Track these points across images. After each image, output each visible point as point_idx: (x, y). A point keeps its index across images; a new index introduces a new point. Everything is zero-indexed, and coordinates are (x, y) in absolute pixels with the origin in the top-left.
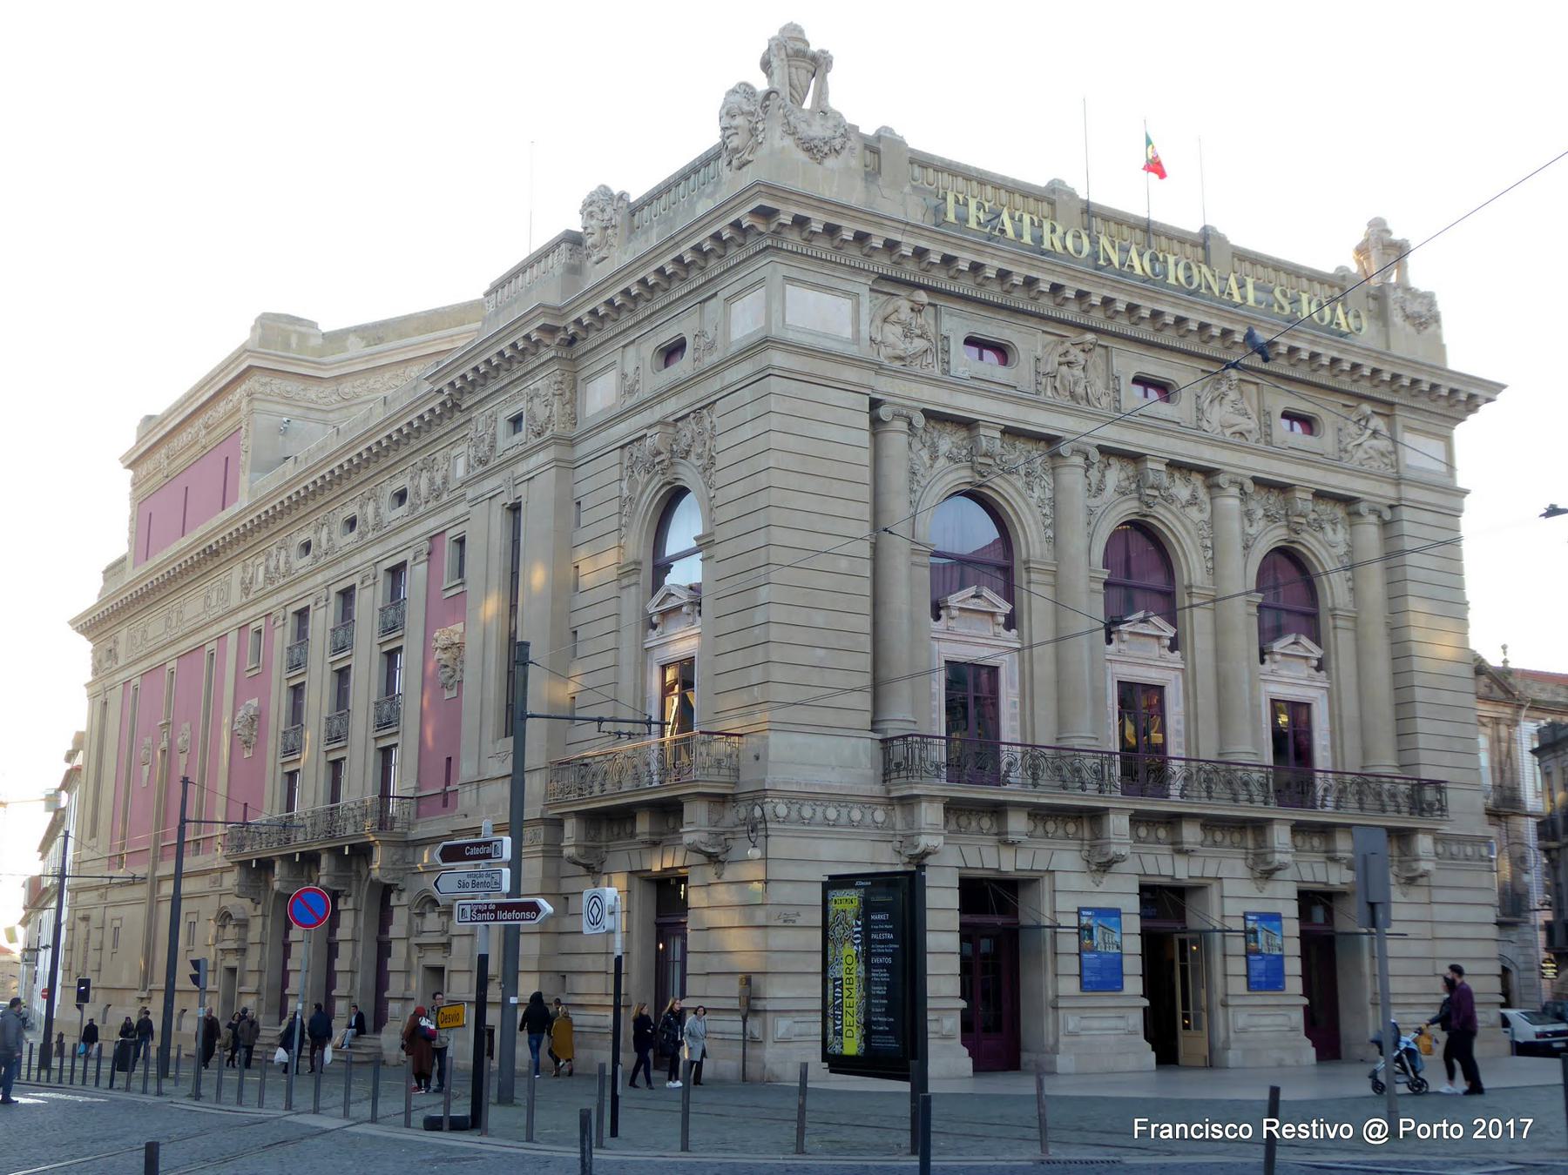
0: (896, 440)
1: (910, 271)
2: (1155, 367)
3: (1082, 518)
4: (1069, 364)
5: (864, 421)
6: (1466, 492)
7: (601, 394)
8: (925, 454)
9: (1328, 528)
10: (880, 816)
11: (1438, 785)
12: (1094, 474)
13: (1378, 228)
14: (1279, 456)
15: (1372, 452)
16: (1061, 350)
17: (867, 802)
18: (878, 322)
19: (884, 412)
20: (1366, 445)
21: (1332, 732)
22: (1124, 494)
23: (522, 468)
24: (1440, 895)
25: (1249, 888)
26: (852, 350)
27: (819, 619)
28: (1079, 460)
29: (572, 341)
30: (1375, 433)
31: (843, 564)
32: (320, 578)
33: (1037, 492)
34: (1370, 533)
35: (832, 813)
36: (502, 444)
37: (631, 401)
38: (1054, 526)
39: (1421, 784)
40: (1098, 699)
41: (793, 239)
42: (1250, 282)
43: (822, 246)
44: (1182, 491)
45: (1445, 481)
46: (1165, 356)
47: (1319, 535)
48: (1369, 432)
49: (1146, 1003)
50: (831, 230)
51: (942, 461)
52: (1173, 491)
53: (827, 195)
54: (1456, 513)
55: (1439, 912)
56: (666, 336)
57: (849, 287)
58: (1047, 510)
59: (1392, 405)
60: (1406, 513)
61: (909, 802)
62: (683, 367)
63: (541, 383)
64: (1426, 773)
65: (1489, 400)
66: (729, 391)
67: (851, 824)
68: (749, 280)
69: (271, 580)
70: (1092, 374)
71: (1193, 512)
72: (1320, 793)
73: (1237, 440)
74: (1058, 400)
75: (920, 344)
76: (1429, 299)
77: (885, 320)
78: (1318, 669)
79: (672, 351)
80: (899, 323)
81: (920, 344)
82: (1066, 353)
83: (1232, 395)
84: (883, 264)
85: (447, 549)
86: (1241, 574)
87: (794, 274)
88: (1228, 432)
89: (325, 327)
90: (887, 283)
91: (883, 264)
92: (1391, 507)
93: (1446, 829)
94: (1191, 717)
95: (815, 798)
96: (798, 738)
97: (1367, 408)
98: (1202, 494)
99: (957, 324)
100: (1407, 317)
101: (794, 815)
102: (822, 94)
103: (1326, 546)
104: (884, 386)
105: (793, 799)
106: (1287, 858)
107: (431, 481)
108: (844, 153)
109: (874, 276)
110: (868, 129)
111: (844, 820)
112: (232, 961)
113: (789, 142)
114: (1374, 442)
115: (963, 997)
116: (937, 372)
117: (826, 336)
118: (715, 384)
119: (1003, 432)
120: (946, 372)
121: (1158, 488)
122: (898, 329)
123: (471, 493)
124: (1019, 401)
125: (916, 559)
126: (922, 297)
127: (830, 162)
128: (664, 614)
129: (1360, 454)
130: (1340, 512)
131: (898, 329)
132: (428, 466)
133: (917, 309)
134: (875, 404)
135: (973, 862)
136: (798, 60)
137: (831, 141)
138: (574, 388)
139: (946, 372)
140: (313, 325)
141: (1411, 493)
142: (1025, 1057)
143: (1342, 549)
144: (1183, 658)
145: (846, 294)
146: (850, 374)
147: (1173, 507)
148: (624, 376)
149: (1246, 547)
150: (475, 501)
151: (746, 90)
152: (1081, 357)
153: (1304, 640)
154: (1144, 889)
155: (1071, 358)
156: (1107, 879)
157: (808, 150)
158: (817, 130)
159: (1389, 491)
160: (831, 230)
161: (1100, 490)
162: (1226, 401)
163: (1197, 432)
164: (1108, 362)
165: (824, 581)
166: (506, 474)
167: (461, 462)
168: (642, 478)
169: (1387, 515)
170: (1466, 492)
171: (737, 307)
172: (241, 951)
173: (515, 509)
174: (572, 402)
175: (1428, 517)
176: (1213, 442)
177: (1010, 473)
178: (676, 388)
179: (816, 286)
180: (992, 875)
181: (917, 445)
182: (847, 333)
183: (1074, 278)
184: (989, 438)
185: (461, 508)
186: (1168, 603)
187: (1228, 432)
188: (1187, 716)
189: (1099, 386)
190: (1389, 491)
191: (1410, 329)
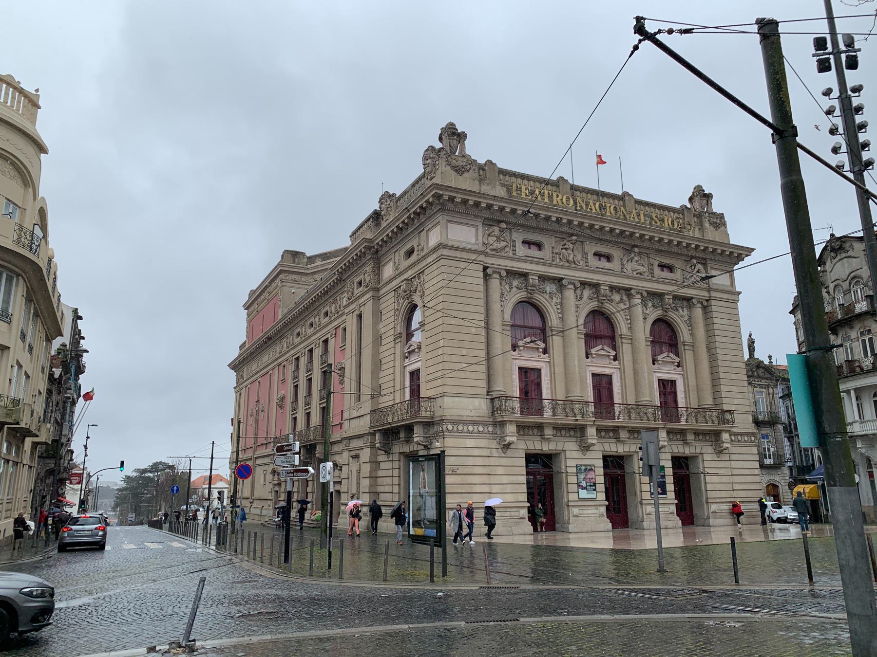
0: (495, 283)
1: (497, 216)
3: (573, 309)
4: (566, 249)
5: (481, 274)
6: (740, 293)
7: (388, 271)
8: (507, 287)
9: (680, 310)
10: (491, 429)
11: (730, 412)
12: (578, 291)
14: (657, 282)
16: (562, 243)
17: (485, 424)
18: (486, 236)
19: (489, 271)
21: (685, 391)
23: (362, 300)
24: (733, 457)
25: (575, 454)
26: (476, 247)
27: (464, 352)
28: (571, 286)
29: (377, 251)
30: (698, 272)
32: (302, 345)
33: (555, 300)
34: (698, 312)
35: (471, 428)
36: (356, 292)
37: (397, 272)
38: (562, 313)
39: (724, 412)
40: (583, 381)
41: (450, 206)
42: (642, 213)
43: (461, 208)
44: (616, 297)
45: (730, 289)
46: (606, 243)
48: (696, 269)
49: (528, 505)
50: (465, 202)
51: (514, 289)
52: (613, 297)
53: (464, 188)
54: (736, 302)
55: (734, 464)
56: (407, 247)
57: (473, 223)
58: (559, 306)
59: (705, 259)
60: (713, 302)
61: (502, 424)
62: (414, 257)
63: (368, 268)
64: (725, 408)
65: (747, 256)
66: (428, 266)
67: (479, 432)
68: (435, 223)
69: (288, 347)
70: (576, 252)
72: (617, 413)
73: (639, 275)
74: (562, 263)
75: (503, 244)
76: (721, 216)
77: (489, 235)
78: (678, 366)
79: (410, 253)
80: (494, 236)
81: (503, 244)
83: (636, 258)
84: (487, 214)
85: (340, 331)
86: (643, 331)
87: (451, 219)
89: (308, 255)
90: (490, 222)
91: (487, 214)
92: (707, 300)
93: (735, 430)
94: (624, 387)
95: (465, 423)
96: (457, 399)
97: (695, 261)
98: (625, 298)
99: (518, 236)
100: (711, 224)
101: (455, 429)
102: (463, 149)
103: (679, 318)
104: (489, 261)
105: (455, 422)
106: (666, 443)
107: (336, 307)
110: (482, 161)
111: (476, 430)
112: (277, 488)
113: (448, 168)
115: (528, 502)
116: (511, 254)
118: (424, 263)
119: (539, 277)
120: (514, 254)
121: (606, 296)
122: (495, 239)
123: (346, 311)
124: (545, 264)
125: (505, 328)
126: (504, 225)
127: (466, 175)
128: (409, 353)
130: (685, 303)
131: (495, 239)
132: (335, 302)
133: (502, 230)
134: (485, 268)
135: (531, 447)
137: (464, 166)
138: (379, 270)
139: (514, 254)
140: (303, 254)
141: (714, 294)
142: (557, 525)
143: (686, 318)
144: (549, 357)
145: (473, 226)
148: (395, 263)
149: (645, 318)
150: (348, 314)
151: (431, 148)
152: (571, 246)
153: (671, 355)
154: (604, 456)
156: (588, 453)
157: (456, 171)
158: (460, 163)
160: (465, 202)
161: (581, 298)
163: (622, 274)
164: (583, 248)
165: (466, 337)
166: (356, 303)
167: (345, 300)
168: (401, 301)
169: (705, 303)
170: (740, 293)
171: (431, 233)
172: (279, 485)
173: (360, 316)
174: (378, 274)
175: (723, 304)
176: (628, 277)
178: (411, 267)
179: (460, 223)
180: (540, 452)
181: (503, 283)
182: (473, 241)
183: (566, 215)
184: (533, 280)
185: (344, 317)
186: (543, 332)
188: (622, 386)
189: (579, 257)
190: (706, 294)
191: (712, 228)
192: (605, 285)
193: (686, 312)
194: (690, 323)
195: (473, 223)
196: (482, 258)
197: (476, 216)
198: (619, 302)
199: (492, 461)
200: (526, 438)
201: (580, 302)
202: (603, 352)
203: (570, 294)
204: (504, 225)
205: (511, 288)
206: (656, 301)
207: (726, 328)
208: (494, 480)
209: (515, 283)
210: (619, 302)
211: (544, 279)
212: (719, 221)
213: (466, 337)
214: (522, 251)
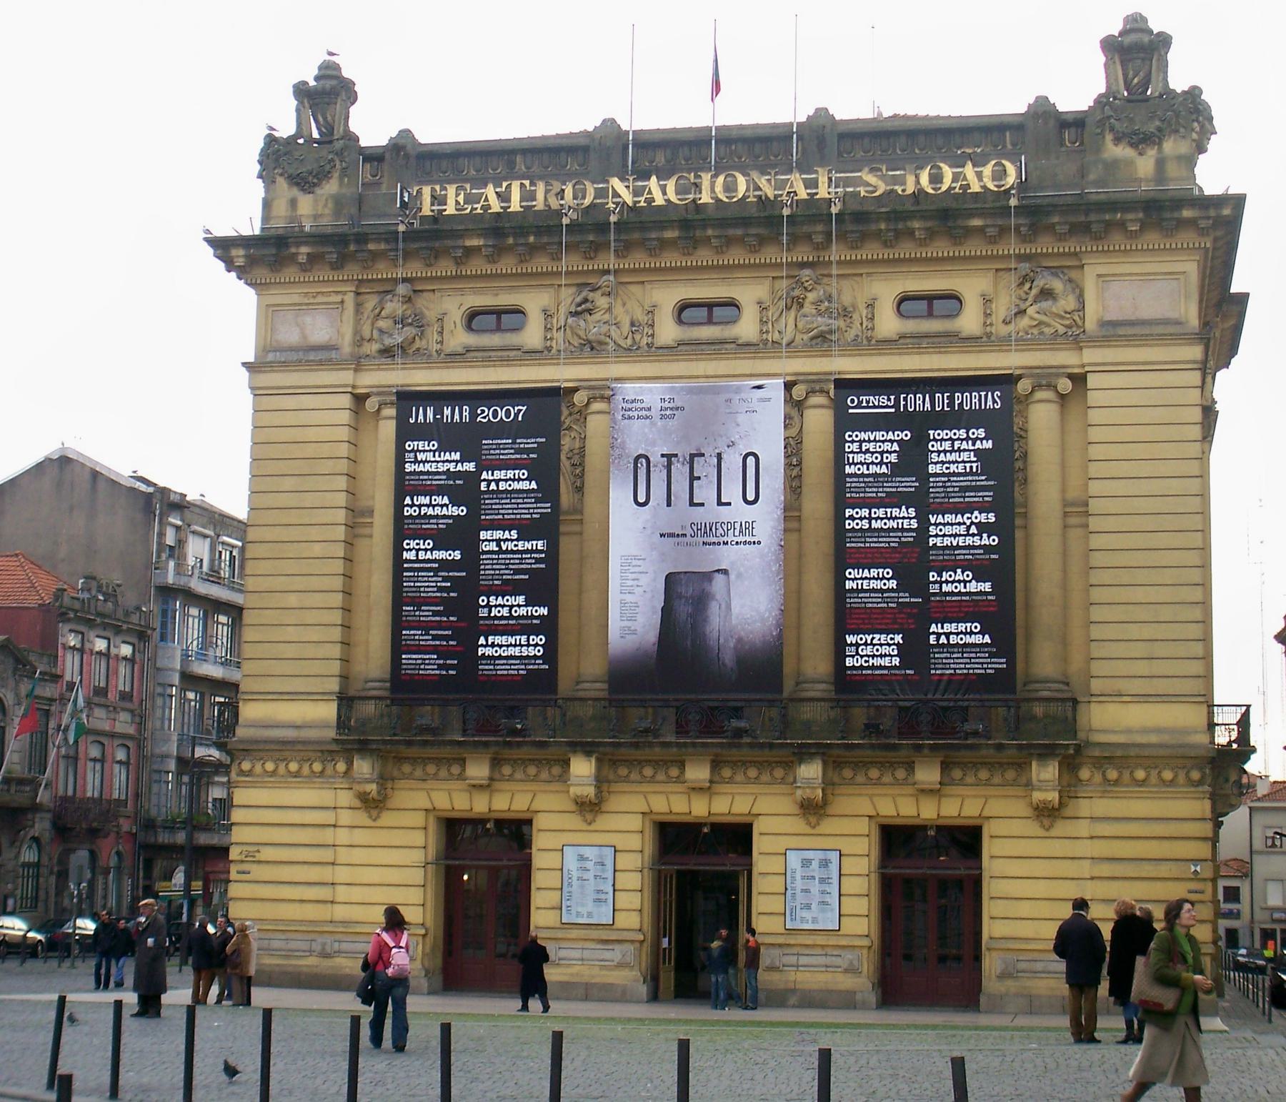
4: (590, 312)
5: (345, 417)
13: (1136, 24)
15: (1044, 318)
16: (578, 299)
19: (371, 404)
30: (1046, 294)
31: (317, 550)
48: (1034, 291)
59: (1075, 254)
82: (586, 300)
114: (1045, 305)
126: (402, 289)
129: (1024, 322)
136: (327, 94)
152: (602, 302)
155: (588, 305)
196: (346, 377)
199: (343, 836)
200: (430, 784)
204: (402, 289)
208: (342, 874)
212: (1190, 117)
214: (459, 338)
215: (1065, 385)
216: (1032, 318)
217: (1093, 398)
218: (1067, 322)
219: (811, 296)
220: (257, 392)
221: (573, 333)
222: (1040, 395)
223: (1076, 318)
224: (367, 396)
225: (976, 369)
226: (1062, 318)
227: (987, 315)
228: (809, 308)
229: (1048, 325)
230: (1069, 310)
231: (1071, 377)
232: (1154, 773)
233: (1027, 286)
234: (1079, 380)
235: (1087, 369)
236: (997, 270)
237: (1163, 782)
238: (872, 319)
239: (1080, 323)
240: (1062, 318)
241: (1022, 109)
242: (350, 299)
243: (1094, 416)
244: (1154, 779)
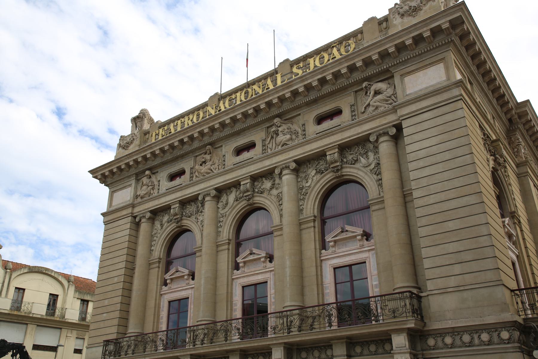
1: (141, 167)
2: (242, 141)
4: (205, 162)
20: (371, 104)
22: (237, 200)
27: (106, 302)
30: (377, 93)
31: (116, 280)
44: (267, 184)
47: (357, 165)
48: (372, 93)
51: (166, 224)
57: (129, 183)
59: (387, 71)
71: (275, 192)
84: (133, 171)
87: (115, 189)
88: (280, 147)
99: (163, 175)
108: (135, 141)
109: (134, 176)
113: (121, 149)
114: (379, 97)
117: (122, 203)
126: (147, 172)
129: (371, 109)
146: (124, 212)
147: (265, 195)
152: (208, 157)
159: (392, 118)
161: (227, 204)
162: (280, 133)
177: (189, 217)
187: (280, 147)
192: (245, 179)
193: (371, 155)
194: (377, 171)
195: (129, 183)
196: (129, 210)
197: (129, 177)
198: (271, 189)
201: (226, 210)
202: (251, 257)
203: (209, 206)
204: (147, 172)
205: (162, 225)
206: (322, 165)
207: (434, 150)
209: (166, 218)
210: (271, 189)
211: (185, 203)
213: (110, 288)
215: (394, 131)
216: (373, 106)
217: (406, 132)
218: (389, 102)
219: (280, 129)
220: (106, 223)
221: (198, 172)
222: (381, 139)
223: (393, 98)
224: (137, 216)
225: (349, 137)
226: (387, 101)
227: (352, 111)
228: (281, 134)
229: (381, 106)
230: (388, 95)
231: (394, 126)
232: (476, 336)
233: (368, 94)
234: (399, 128)
235: (401, 119)
236: (356, 92)
237: (482, 343)
238: (304, 130)
239: (395, 100)
240: (387, 101)
241: (360, 25)
242: (133, 182)
243: (407, 140)
244: (476, 341)
